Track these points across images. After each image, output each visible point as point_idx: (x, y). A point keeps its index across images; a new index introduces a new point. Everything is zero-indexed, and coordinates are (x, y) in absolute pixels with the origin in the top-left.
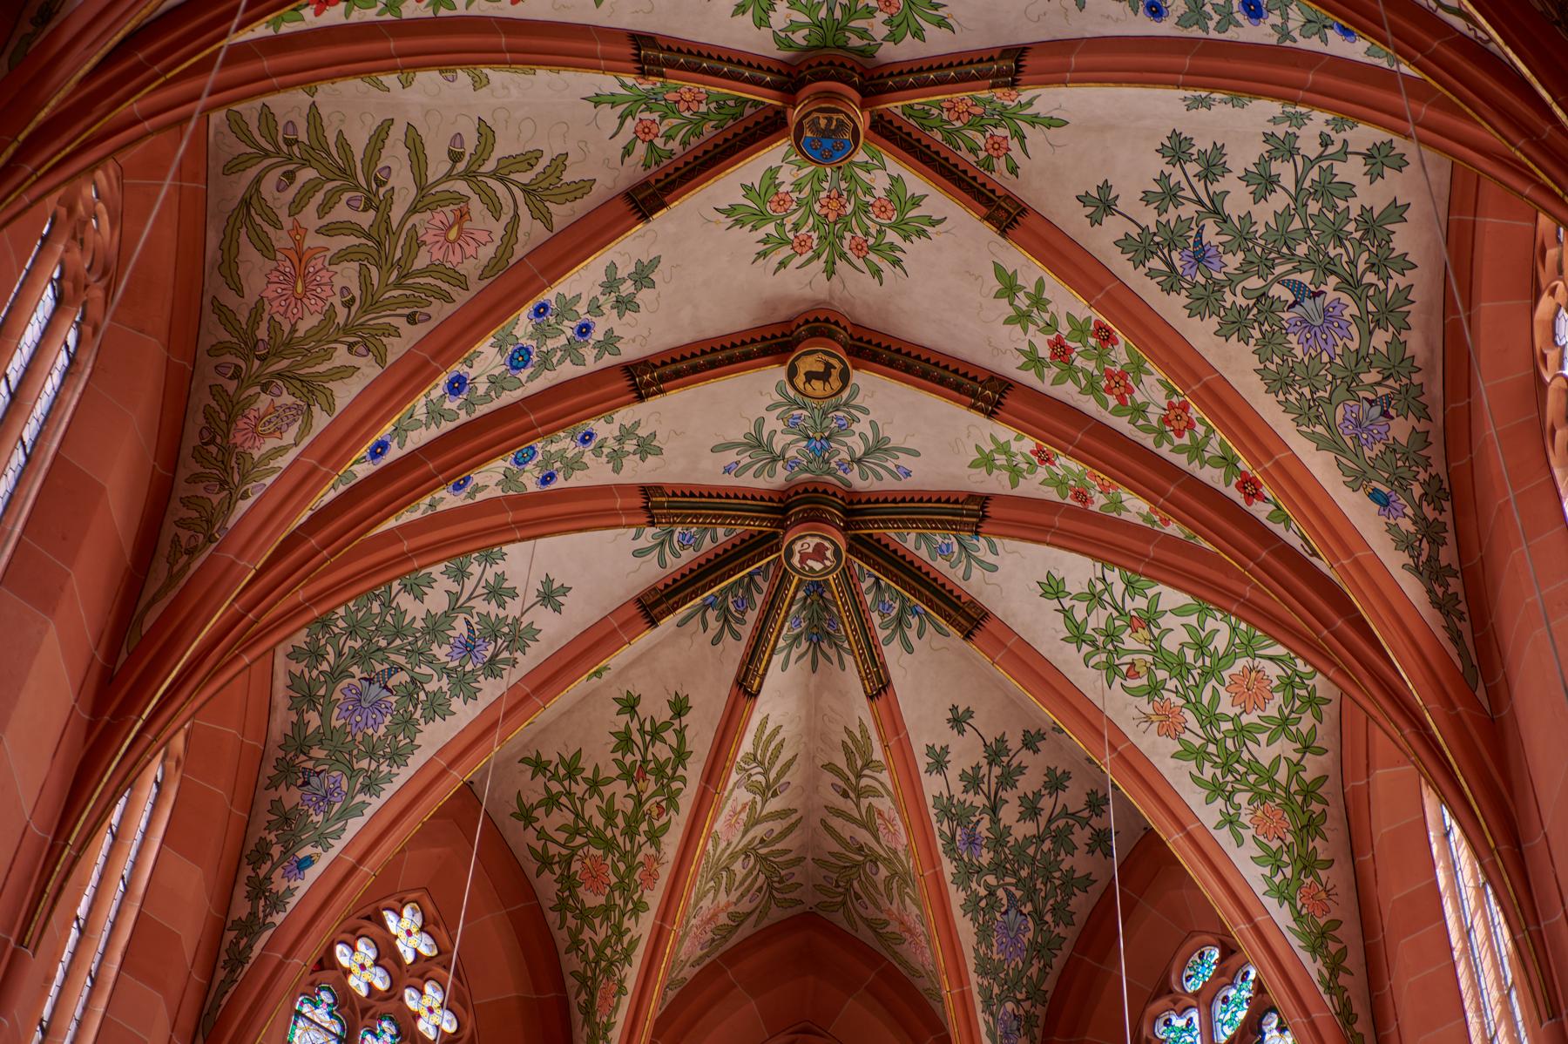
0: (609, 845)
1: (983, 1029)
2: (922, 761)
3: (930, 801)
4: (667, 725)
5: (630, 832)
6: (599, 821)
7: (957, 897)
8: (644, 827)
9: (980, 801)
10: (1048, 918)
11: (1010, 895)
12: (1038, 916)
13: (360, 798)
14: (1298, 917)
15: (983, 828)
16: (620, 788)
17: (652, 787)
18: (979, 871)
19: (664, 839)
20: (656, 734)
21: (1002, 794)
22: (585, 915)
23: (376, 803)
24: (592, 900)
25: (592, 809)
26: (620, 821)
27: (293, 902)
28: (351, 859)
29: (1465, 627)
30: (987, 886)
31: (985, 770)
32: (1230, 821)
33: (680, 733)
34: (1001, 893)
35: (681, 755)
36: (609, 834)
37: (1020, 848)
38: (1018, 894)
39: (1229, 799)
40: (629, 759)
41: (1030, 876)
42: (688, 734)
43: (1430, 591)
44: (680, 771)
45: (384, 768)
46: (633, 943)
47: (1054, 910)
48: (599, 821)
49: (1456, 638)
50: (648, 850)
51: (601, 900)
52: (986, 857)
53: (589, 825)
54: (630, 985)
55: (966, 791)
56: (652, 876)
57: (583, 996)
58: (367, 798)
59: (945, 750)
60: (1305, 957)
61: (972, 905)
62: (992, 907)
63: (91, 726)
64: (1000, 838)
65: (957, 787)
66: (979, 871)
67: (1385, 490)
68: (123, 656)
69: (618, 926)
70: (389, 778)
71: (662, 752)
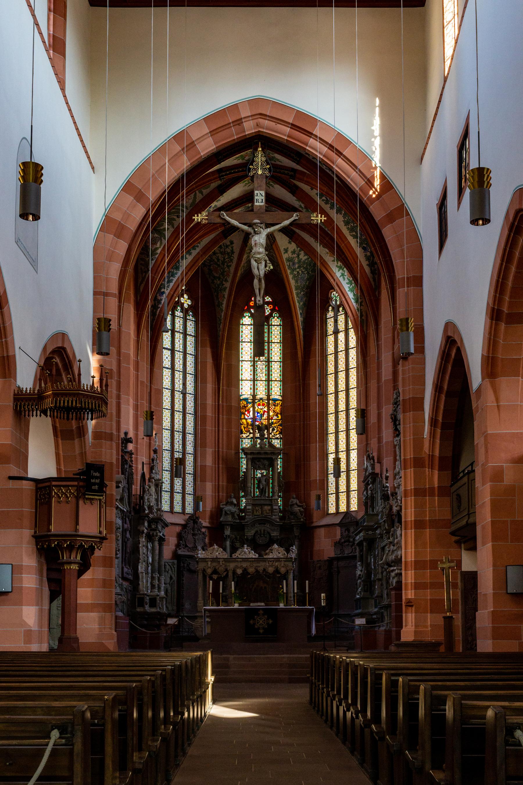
0: (219, 265)
1: (296, 301)
2: (283, 251)
3: (285, 259)
4: (229, 245)
5: (223, 263)
6: (216, 260)
7: (290, 277)
8: (226, 264)
9: (295, 255)
10: (310, 273)
11: (302, 271)
12: (308, 273)
13: (171, 278)
14: (354, 295)
15: (296, 261)
16: (220, 255)
17: (227, 257)
18: (296, 269)
19: (230, 268)
20: (227, 246)
21: (300, 253)
22: (214, 277)
23: (175, 280)
24: (216, 275)
25: (214, 257)
26: (220, 261)
27: (163, 302)
28: (172, 293)
29: (376, 276)
30: (297, 271)
31: (296, 249)
32: (343, 275)
33: (232, 247)
34: (300, 272)
35: (233, 252)
36: (218, 263)
37: (304, 262)
38: (304, 270)
39: (343, 270)
40: (222, 250)
41: (306, 266)
42: (234, 248)
43: (371, 270)
44: (233, 255)
45: (175, 271)
46: (225, 288)
47: (311, 271)
48: (216, 260)
49: (374, 280)
50: (226, 269)
51: (218, 276)
52: (297, 266)
53: (214, 260)
54: (226, 296)
55: (292, 255)
56: (228, 275)
57: (216, 294)
58: (173, 278)
59: (288, 248)
60: (354, 304)
61: (294, 277)
62: (298, 275)
63: (137, 314)
64: (300, 261)
65: (290, 255)
66: (296, 269)
67: (365, 246)
68: (139, 298)
69: (222, 282)
70: (176, 273)
71: (228, 250)
